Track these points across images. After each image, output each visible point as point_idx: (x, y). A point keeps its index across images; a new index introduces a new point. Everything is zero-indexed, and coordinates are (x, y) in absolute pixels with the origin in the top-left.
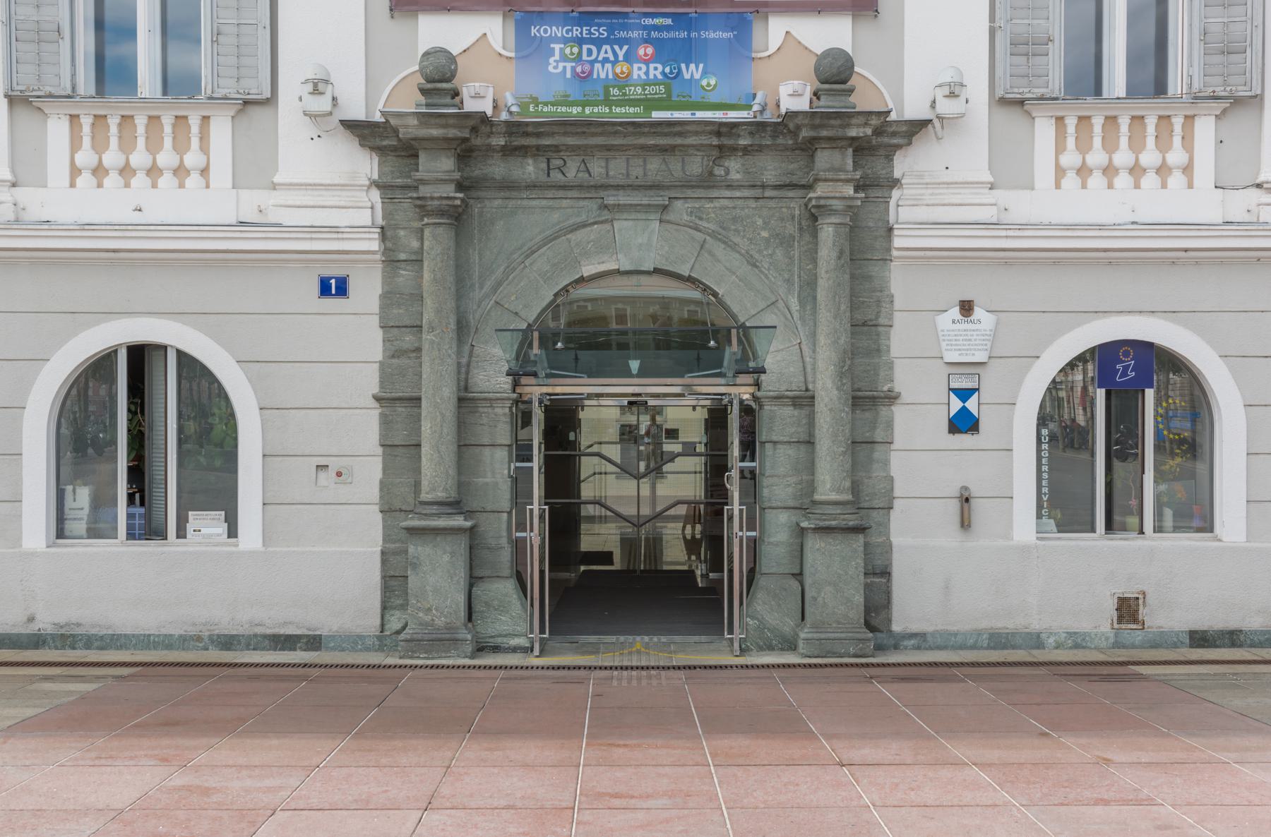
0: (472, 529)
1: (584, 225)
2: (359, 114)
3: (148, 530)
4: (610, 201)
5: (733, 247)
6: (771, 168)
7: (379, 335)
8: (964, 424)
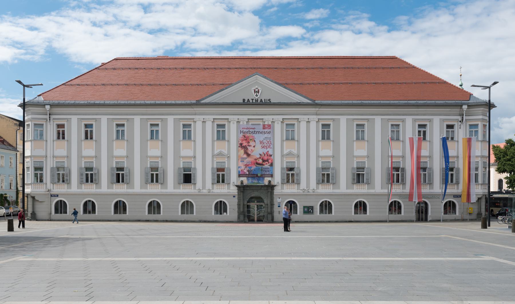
3: (221, 214)
6: (265, 188)
8: (279, 206)
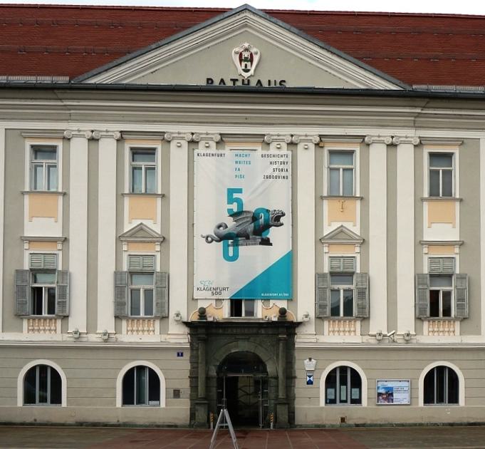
0: (208, 404)
1: (231, 342)
2: (185, 320)
4: (237, 337)
5: (262, 346)
7: (189, 364)
